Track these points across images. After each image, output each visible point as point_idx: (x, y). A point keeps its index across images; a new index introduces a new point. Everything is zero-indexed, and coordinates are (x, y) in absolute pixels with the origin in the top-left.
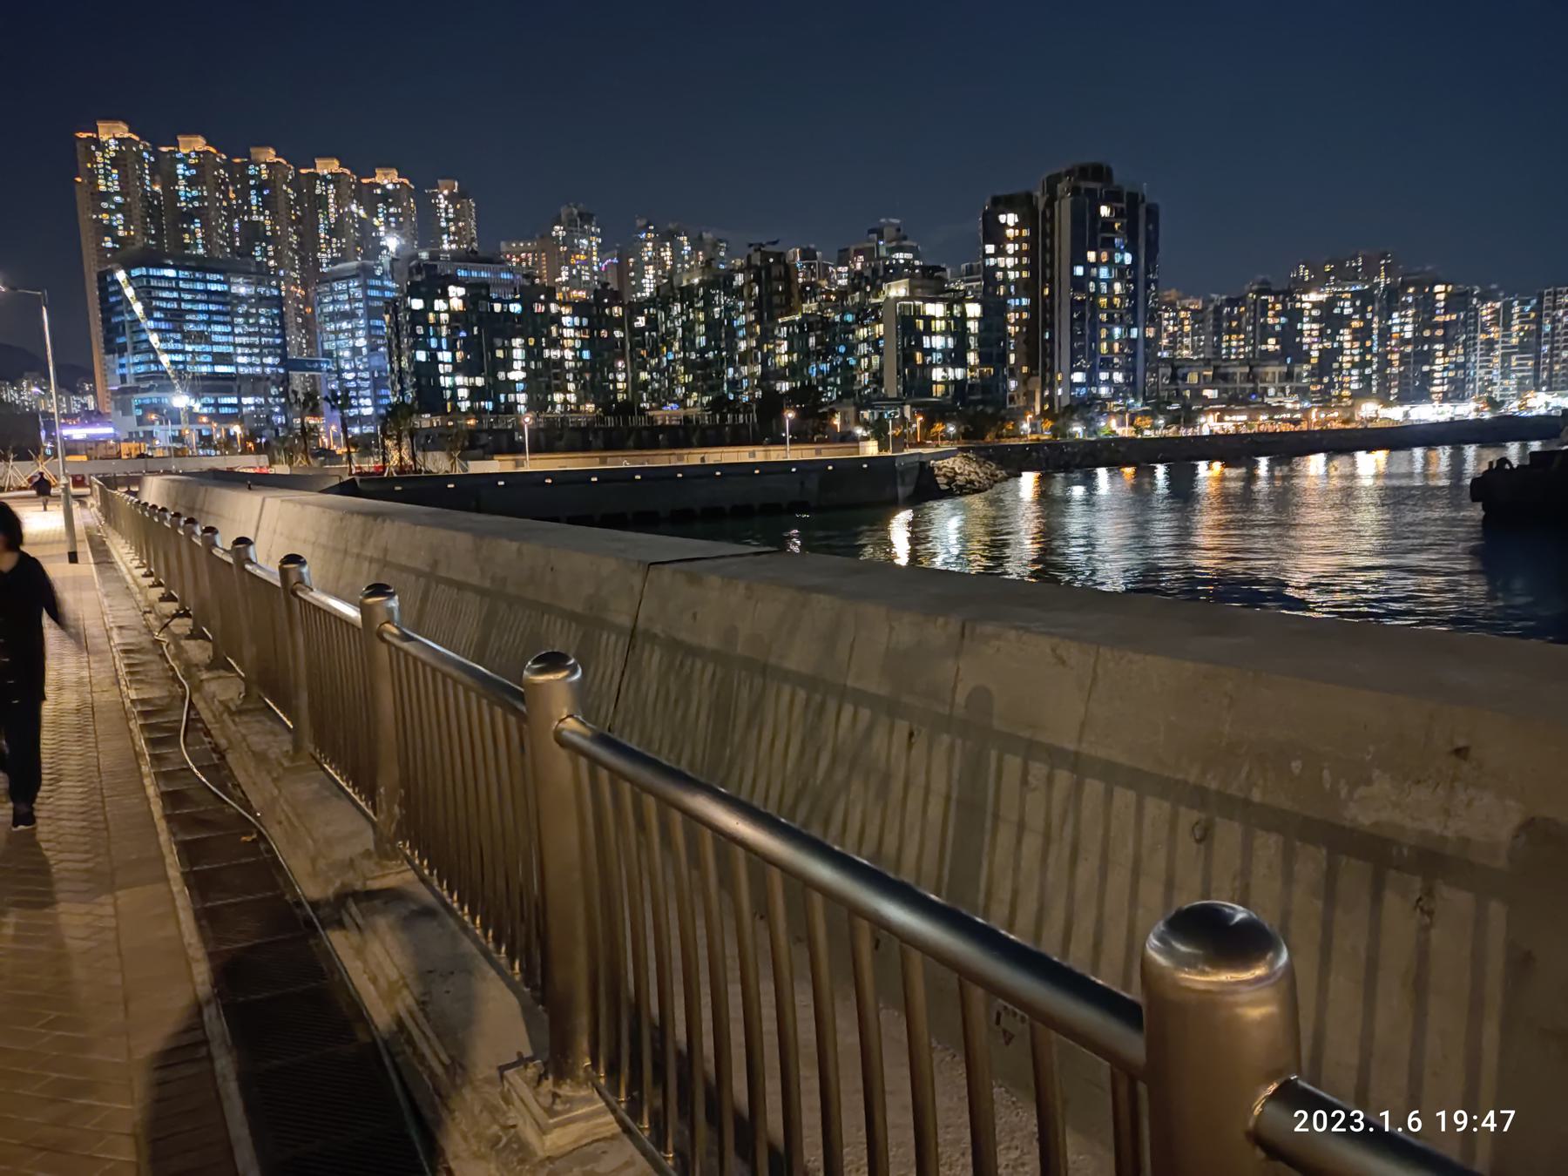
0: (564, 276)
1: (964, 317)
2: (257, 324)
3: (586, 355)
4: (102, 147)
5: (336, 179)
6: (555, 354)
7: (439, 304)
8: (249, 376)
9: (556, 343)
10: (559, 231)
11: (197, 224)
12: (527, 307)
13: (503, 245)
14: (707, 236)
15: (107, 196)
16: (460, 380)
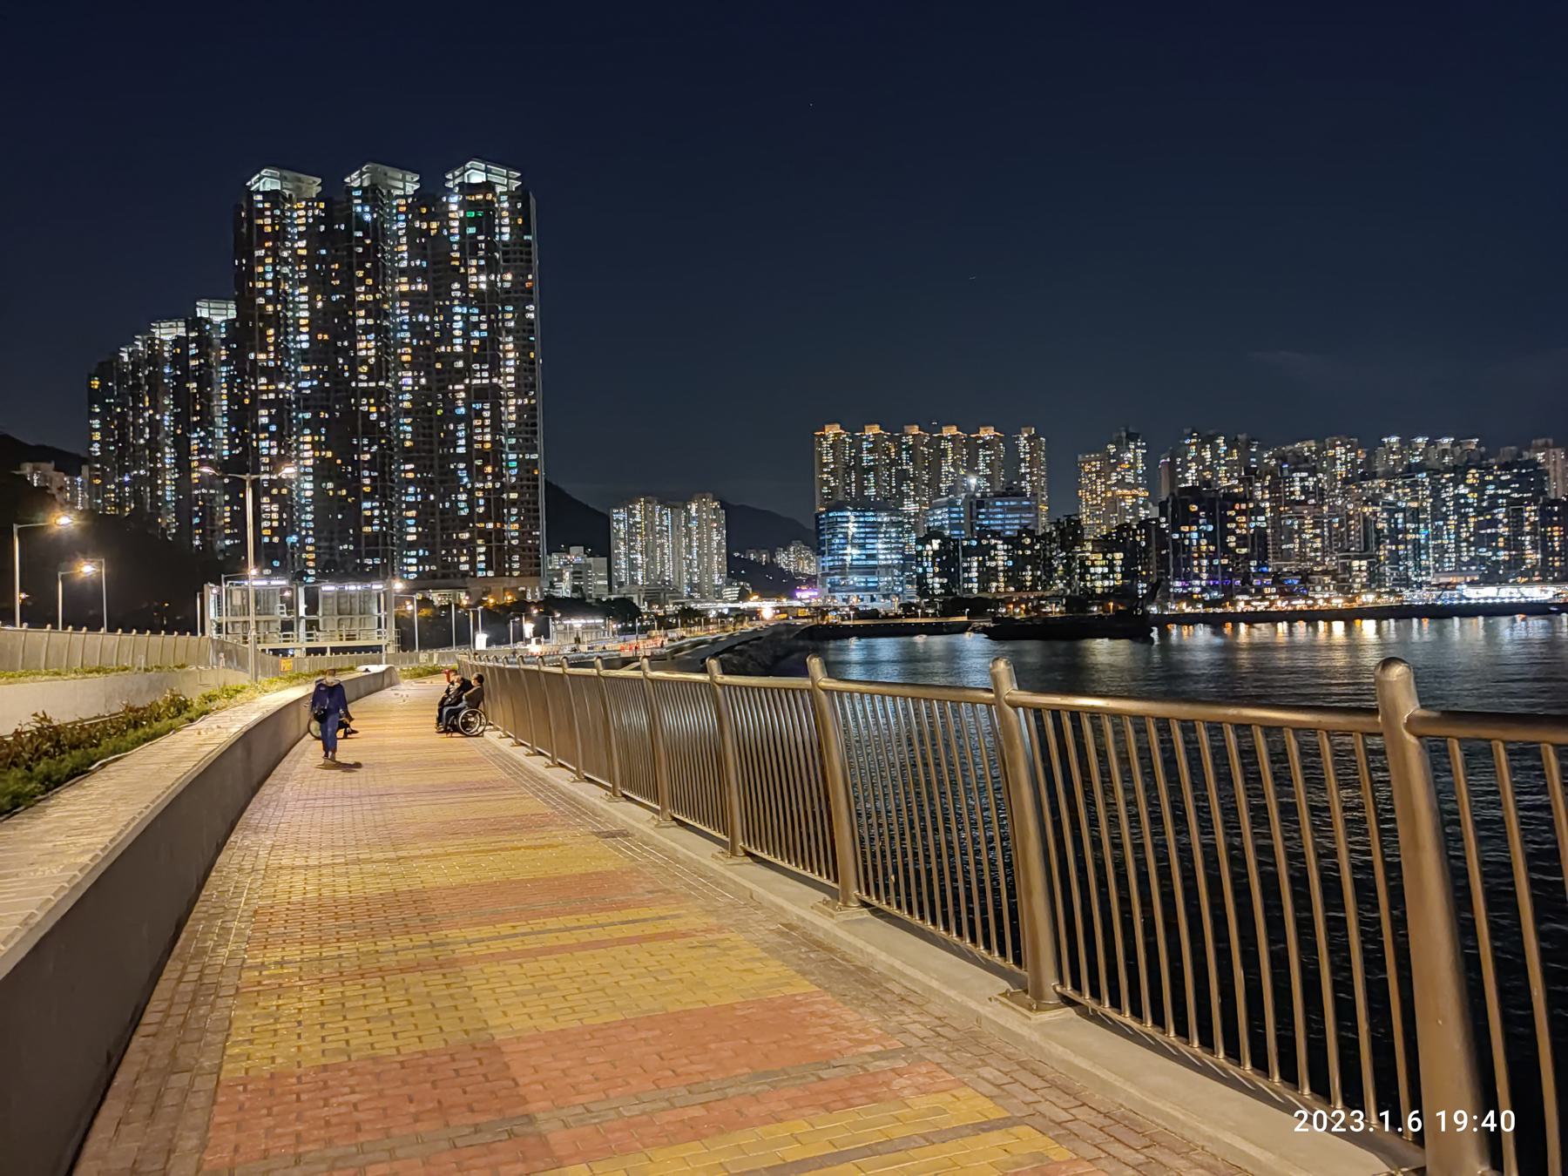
0: (1114, 477)
1: (1113, 559)
2: (890, 537)
3: (1010, 563)
4: (826, 438)
5: (953, 439)
6: (993, 564)
7: (928, 547)
8: (884, 566)
9: (992, 559)
10: (1112, 448)
11: (871, 476)
12: (979, 541)
13: (1080, 457)
14: (1242, 437)
15: (826, 465)
16: (937, 580)
